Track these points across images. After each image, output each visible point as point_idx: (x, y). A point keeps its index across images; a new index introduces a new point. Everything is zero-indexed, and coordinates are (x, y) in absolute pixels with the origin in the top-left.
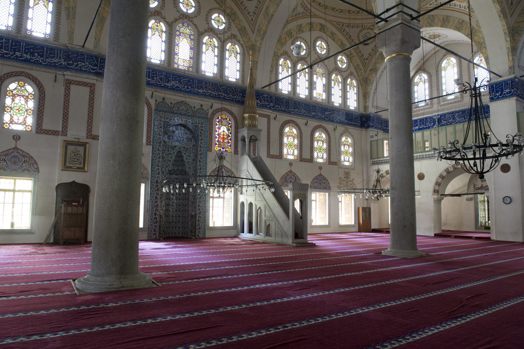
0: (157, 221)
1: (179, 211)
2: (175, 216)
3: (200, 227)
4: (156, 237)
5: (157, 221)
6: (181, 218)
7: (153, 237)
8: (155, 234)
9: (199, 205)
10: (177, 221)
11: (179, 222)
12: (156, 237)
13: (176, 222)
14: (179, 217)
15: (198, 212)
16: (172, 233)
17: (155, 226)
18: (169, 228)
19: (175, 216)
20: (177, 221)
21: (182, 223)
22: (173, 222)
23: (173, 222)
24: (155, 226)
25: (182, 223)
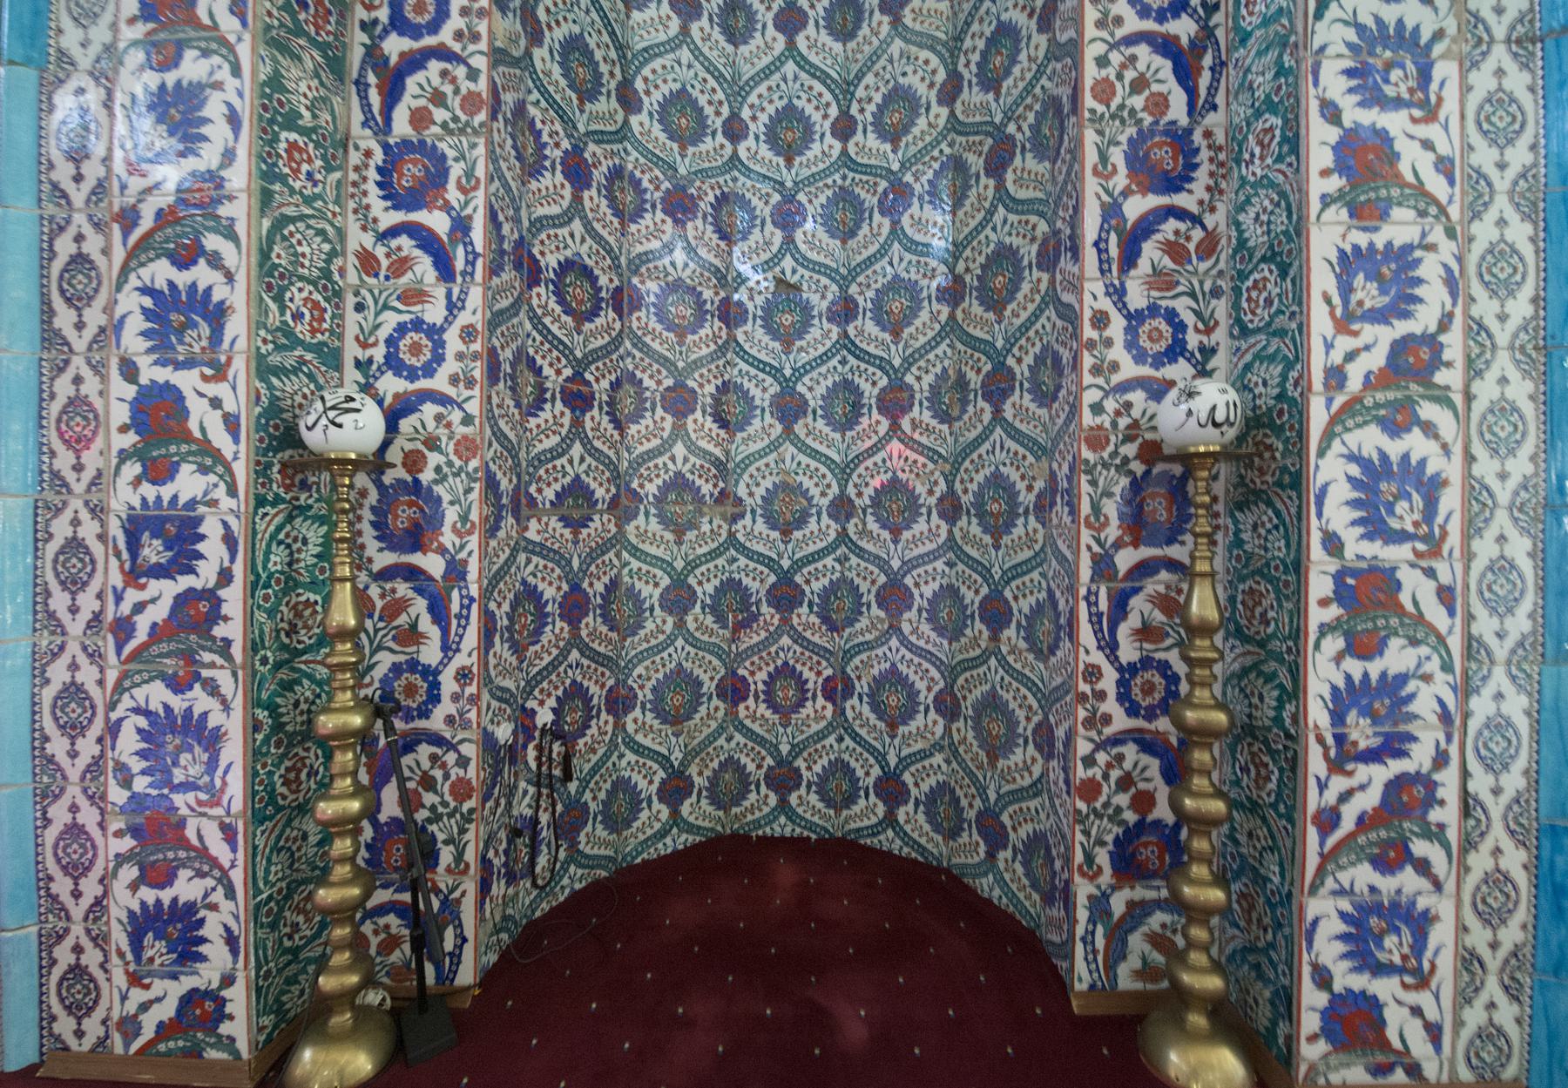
0: (197, 613)
1: (894, 403)
2: (820, 489)
3: (1409, 798)
4: (201, 1011)
5: (197, 613)
6: (927, 530)
7: (115, 995)
8: (179, 930)
9: (1365, 160)
10: (869, 583)
11: (894, 596)
12: (201, 1011)
13: (838, 607)
14: (896, 505)
15: (1341, 348)
16: (784, 779)
17: (165, 732)
18: (733, 690)
19: (820, 489)
20: (869, 583)
21: (948, 613)
22: (786, 595)
23: (786, 595)
24: (173, 732)
25: (948, 613)
